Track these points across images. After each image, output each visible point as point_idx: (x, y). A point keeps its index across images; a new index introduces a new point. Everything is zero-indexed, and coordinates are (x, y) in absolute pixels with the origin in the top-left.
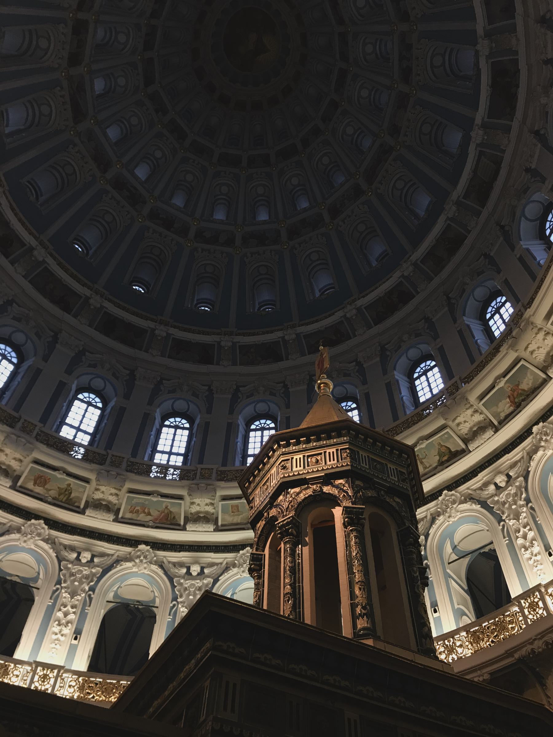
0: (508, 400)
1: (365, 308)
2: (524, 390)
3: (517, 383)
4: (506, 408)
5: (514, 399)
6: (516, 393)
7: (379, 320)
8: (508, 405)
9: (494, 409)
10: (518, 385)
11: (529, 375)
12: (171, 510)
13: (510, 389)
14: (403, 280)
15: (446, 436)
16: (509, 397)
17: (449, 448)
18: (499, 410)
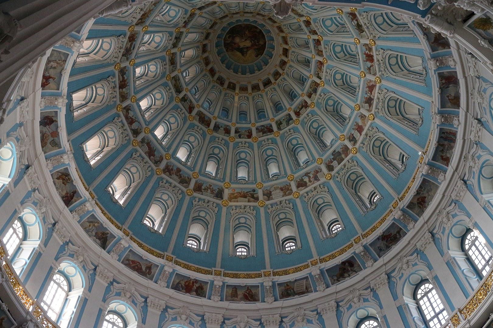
7: (176, 287)
12: (3, 323)
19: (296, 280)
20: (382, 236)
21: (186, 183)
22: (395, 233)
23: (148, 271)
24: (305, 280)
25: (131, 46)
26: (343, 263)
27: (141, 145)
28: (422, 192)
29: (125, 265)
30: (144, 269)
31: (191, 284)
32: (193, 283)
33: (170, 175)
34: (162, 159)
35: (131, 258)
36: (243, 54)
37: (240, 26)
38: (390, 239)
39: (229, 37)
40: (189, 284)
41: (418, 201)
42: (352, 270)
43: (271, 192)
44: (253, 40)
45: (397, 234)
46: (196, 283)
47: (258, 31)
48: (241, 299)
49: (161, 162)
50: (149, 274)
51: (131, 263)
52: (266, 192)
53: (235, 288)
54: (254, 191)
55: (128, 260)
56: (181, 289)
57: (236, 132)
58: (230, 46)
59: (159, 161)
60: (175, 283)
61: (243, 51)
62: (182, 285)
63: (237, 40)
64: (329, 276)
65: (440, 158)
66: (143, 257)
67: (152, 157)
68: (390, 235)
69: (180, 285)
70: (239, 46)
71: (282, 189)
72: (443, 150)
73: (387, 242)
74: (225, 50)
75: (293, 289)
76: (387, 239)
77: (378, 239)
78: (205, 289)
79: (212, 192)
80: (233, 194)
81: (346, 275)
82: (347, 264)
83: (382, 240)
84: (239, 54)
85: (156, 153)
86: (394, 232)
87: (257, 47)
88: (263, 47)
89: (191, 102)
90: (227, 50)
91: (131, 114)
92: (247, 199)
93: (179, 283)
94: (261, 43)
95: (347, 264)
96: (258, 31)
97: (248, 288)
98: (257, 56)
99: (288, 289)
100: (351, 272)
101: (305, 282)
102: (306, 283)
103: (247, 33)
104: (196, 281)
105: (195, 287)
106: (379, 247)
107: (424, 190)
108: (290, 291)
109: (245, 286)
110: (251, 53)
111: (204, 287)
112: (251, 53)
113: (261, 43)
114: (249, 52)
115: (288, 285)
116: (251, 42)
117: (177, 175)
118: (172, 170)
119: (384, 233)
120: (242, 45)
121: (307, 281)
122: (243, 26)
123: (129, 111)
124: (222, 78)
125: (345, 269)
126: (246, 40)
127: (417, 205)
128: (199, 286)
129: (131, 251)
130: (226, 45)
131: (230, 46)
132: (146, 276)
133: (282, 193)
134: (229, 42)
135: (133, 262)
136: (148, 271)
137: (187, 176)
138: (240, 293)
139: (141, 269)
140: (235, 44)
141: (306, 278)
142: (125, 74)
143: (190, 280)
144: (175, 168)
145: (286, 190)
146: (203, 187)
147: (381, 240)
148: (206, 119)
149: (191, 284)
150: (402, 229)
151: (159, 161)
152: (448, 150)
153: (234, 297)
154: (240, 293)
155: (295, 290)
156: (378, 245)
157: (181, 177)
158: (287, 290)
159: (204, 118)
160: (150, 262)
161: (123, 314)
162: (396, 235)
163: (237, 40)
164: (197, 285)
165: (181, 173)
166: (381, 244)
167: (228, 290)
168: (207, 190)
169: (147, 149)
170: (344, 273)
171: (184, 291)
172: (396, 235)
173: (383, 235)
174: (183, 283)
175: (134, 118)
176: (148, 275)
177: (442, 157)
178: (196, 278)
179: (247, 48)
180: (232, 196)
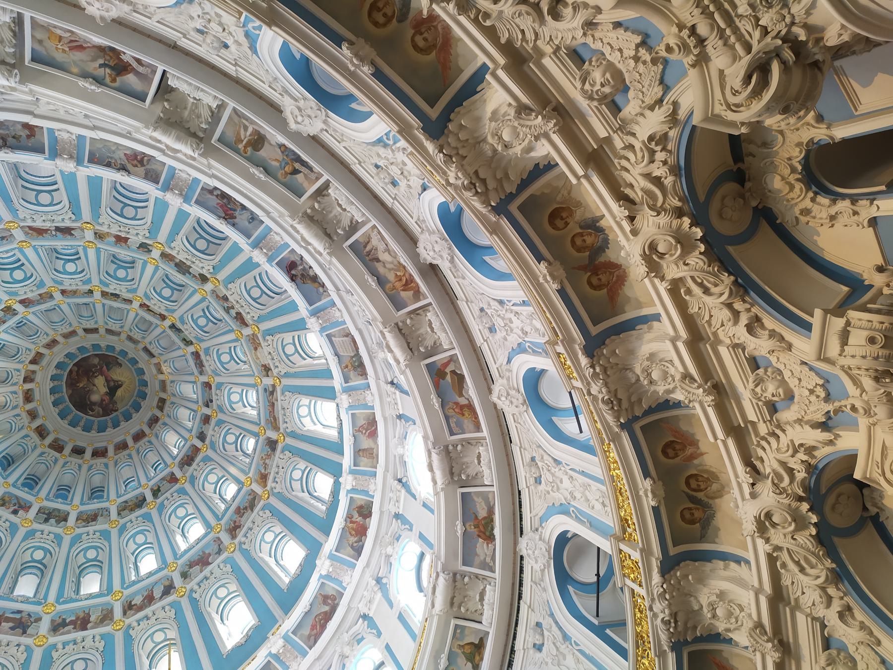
0: (481, 540)
1: (336, 551)
2: (485, 518)
3: (473, 516)
4: (486, 551)
5: (484, 533)
6: (481, 528)
8: (485, 545)
9: (477, 561)
10: (476, 517)
11: (476, 499)
13: (473, 527)
14: (352, 495)
15: (458, 631)
16: (479, 536)
17: (472, 643)
18: (482, 558)
19: (337, 354)
20: (226, 219)
21: (255, 498)
22: (215, 197)
23: (330, 602)
24: (333, 339)
25: (8, 620)
26: (293, 278)
27: (187, 580)
28: (119, 162)
29: (315, 642)
30: (326, 608)
31: (354, 526)
32: (351, 522)
33: (239, 527)
34: (219, 539)
35: (306, 631)
36: (120, 386)
37: (70, 397)
38: (229, 204)
39: (93, 410)
40: (353, 529)
41: (139, 166)
42: (302, 264)
43: (263, 366)
44: (94, 373)
45: (215, 193)
46: (352, 517)
47: (76, 369)
48: (376, 443)
49: (222, 543)
50: (335, 599)
51: (315, 631)
52: (264, 373)
53: (358, 452)
54: (265, 390)
55: (310, 636)
56: (361, 543)
57: (207, 406)
58: (107, 408)
59: (219, 545)
60: (352, 552)
61: (113, 388)
62: (356, 542)
63: (95, 398)
64: (320, 300)
65: (33, 139)
66: (306, 610)
67: (210, 560)
68: (221, 206)
69: (355, 545)
70: (107, 394)
71: (256, 349)
72: (14, 137)
73: (235, 210)
74: (115, 414)
75: (352, 357)
76: (231, 209)
77: (234, 225)
78: (363, 503)
79: (269, 456)
80: (272, 423)
81: (311, 273)
82: (293, 272)
83: (235, 218)
84: (119, 393)
85: (207, 552)
86: (213, 201)
87: (105, 367)
88: (101, 357)
89: (163, 479)
90: (117, 410)
91: (138, 600)
92: (275, 403)
93: (352, 547)
94: (96, 361)
95: (293, 272)
96: (76, 369)
97: (359, 431)
98: (120, 365)
99: (352, 366)
100: (305, 265)
101: (337, 339)
102: (339, 337)
103: (81, 385)
104: (349, 517)
105: (360, 519)
106: (250, 223)
107: (111, 158)
108: (355, 362)
109: (354, 436)
110: (117, 374)
111: (359, 503)
112: (117, 374)
113: (96, 361)
114: (115, 377)
115: (347, 367)
116: (96, 377)
117: (243, 514)
118: (235, 522)
119: (220, 217)
120: (103, 390)
121: (334, 336)
122: (70, 392)
123: (133, 603)
124: (150, 419)
125: (302, 275)
126: (94, 385)
127: (148, 167)
128: (358, 512)
129: (294, 633)
130: (107, 411)
131: (107, 408)
132: (338, 604)
133: (259, 349)
134: (101, 410)
135: (313, 627)
136: (330, 602)
137: (247, 497)
138: (366, 443)
139: (325, 613)
140: (102, 400)
141: (329, 337)
142: (64, 620)
143: (348, 527)
144: (235, 517)
145: (254, 343)
146: (263, 471)
147: (236, 221)
148: (190, 453)
149: (354, 526)
150: (202, 187)
151: (219, 545)
152: (8, 129)
153: (372, 454)
154: (366, 443)
155: (353, 354)
156: (247, 223)
157: (246, 508)
158: (355, 368)
159: (188, 456)
160: (315, 597)
161: (375, 663)
162: (217, 196)
163: (95, 398)
164: (356, 515)
165: (242, 508)
166: (242, 219)
167: (362, 464)
168: (266, 464)
169: (198, 568)
170: (308, 275)
171: (363, 538)
172: (217, 196)
173: (224, 218)
174: (353, 539)
175: (145, 594)
176: (336, 602)
177: (29, 137)
178: (345, 516)
179: (107, 380)
180: (274, 424)
